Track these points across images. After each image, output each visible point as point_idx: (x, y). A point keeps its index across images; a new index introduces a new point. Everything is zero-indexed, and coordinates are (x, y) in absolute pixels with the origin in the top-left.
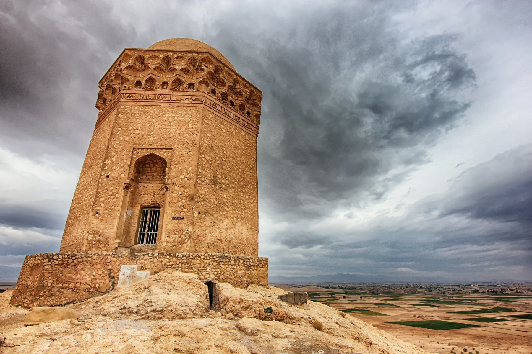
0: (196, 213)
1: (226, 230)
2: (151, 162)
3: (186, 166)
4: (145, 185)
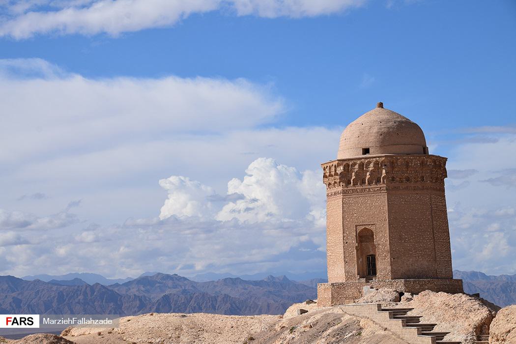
0: (392, 259)
1: (412, 265)
4: (365, 244)
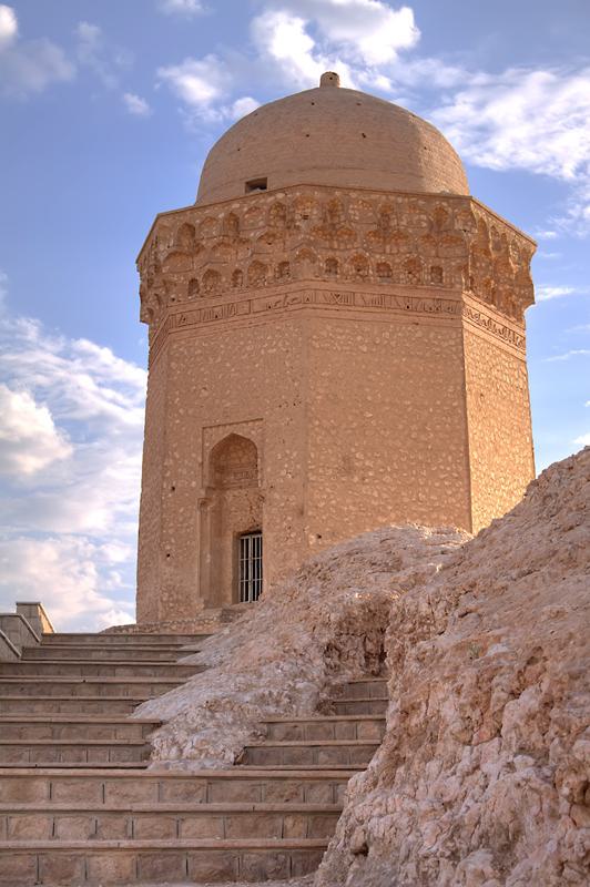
0: (313, 537)
2: (238, 447)
3: (288, 452)
4: (236, 493)
